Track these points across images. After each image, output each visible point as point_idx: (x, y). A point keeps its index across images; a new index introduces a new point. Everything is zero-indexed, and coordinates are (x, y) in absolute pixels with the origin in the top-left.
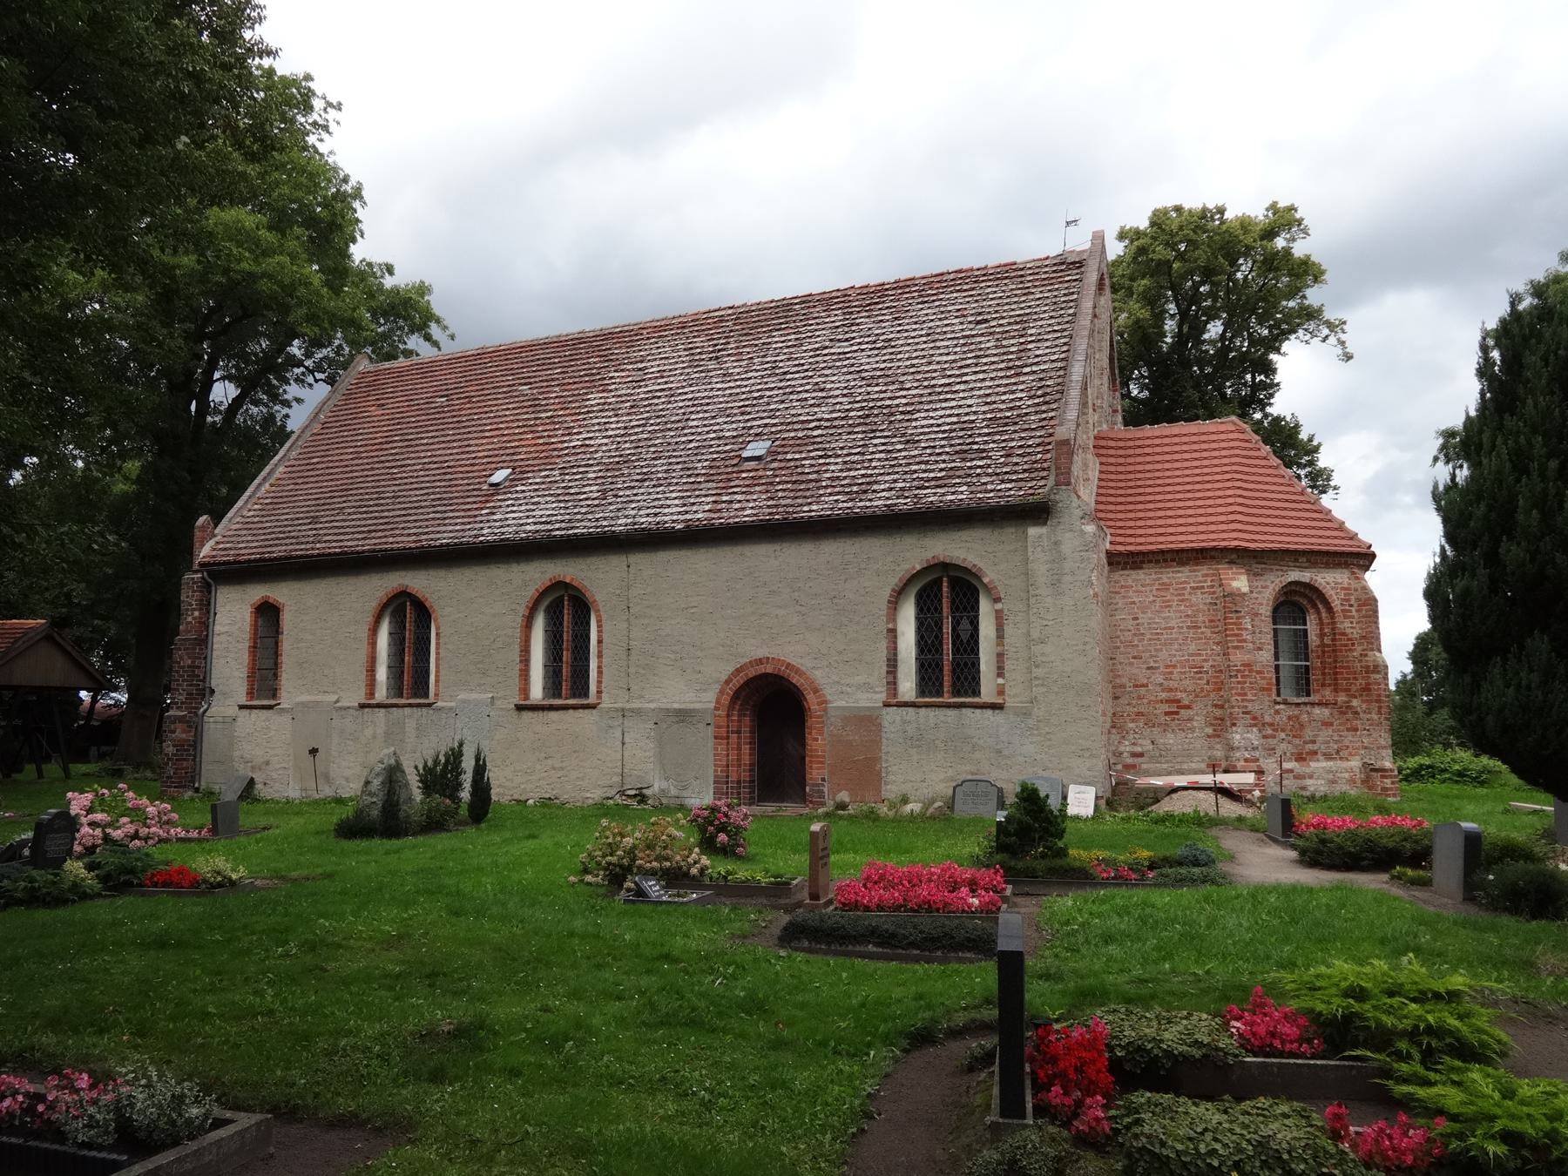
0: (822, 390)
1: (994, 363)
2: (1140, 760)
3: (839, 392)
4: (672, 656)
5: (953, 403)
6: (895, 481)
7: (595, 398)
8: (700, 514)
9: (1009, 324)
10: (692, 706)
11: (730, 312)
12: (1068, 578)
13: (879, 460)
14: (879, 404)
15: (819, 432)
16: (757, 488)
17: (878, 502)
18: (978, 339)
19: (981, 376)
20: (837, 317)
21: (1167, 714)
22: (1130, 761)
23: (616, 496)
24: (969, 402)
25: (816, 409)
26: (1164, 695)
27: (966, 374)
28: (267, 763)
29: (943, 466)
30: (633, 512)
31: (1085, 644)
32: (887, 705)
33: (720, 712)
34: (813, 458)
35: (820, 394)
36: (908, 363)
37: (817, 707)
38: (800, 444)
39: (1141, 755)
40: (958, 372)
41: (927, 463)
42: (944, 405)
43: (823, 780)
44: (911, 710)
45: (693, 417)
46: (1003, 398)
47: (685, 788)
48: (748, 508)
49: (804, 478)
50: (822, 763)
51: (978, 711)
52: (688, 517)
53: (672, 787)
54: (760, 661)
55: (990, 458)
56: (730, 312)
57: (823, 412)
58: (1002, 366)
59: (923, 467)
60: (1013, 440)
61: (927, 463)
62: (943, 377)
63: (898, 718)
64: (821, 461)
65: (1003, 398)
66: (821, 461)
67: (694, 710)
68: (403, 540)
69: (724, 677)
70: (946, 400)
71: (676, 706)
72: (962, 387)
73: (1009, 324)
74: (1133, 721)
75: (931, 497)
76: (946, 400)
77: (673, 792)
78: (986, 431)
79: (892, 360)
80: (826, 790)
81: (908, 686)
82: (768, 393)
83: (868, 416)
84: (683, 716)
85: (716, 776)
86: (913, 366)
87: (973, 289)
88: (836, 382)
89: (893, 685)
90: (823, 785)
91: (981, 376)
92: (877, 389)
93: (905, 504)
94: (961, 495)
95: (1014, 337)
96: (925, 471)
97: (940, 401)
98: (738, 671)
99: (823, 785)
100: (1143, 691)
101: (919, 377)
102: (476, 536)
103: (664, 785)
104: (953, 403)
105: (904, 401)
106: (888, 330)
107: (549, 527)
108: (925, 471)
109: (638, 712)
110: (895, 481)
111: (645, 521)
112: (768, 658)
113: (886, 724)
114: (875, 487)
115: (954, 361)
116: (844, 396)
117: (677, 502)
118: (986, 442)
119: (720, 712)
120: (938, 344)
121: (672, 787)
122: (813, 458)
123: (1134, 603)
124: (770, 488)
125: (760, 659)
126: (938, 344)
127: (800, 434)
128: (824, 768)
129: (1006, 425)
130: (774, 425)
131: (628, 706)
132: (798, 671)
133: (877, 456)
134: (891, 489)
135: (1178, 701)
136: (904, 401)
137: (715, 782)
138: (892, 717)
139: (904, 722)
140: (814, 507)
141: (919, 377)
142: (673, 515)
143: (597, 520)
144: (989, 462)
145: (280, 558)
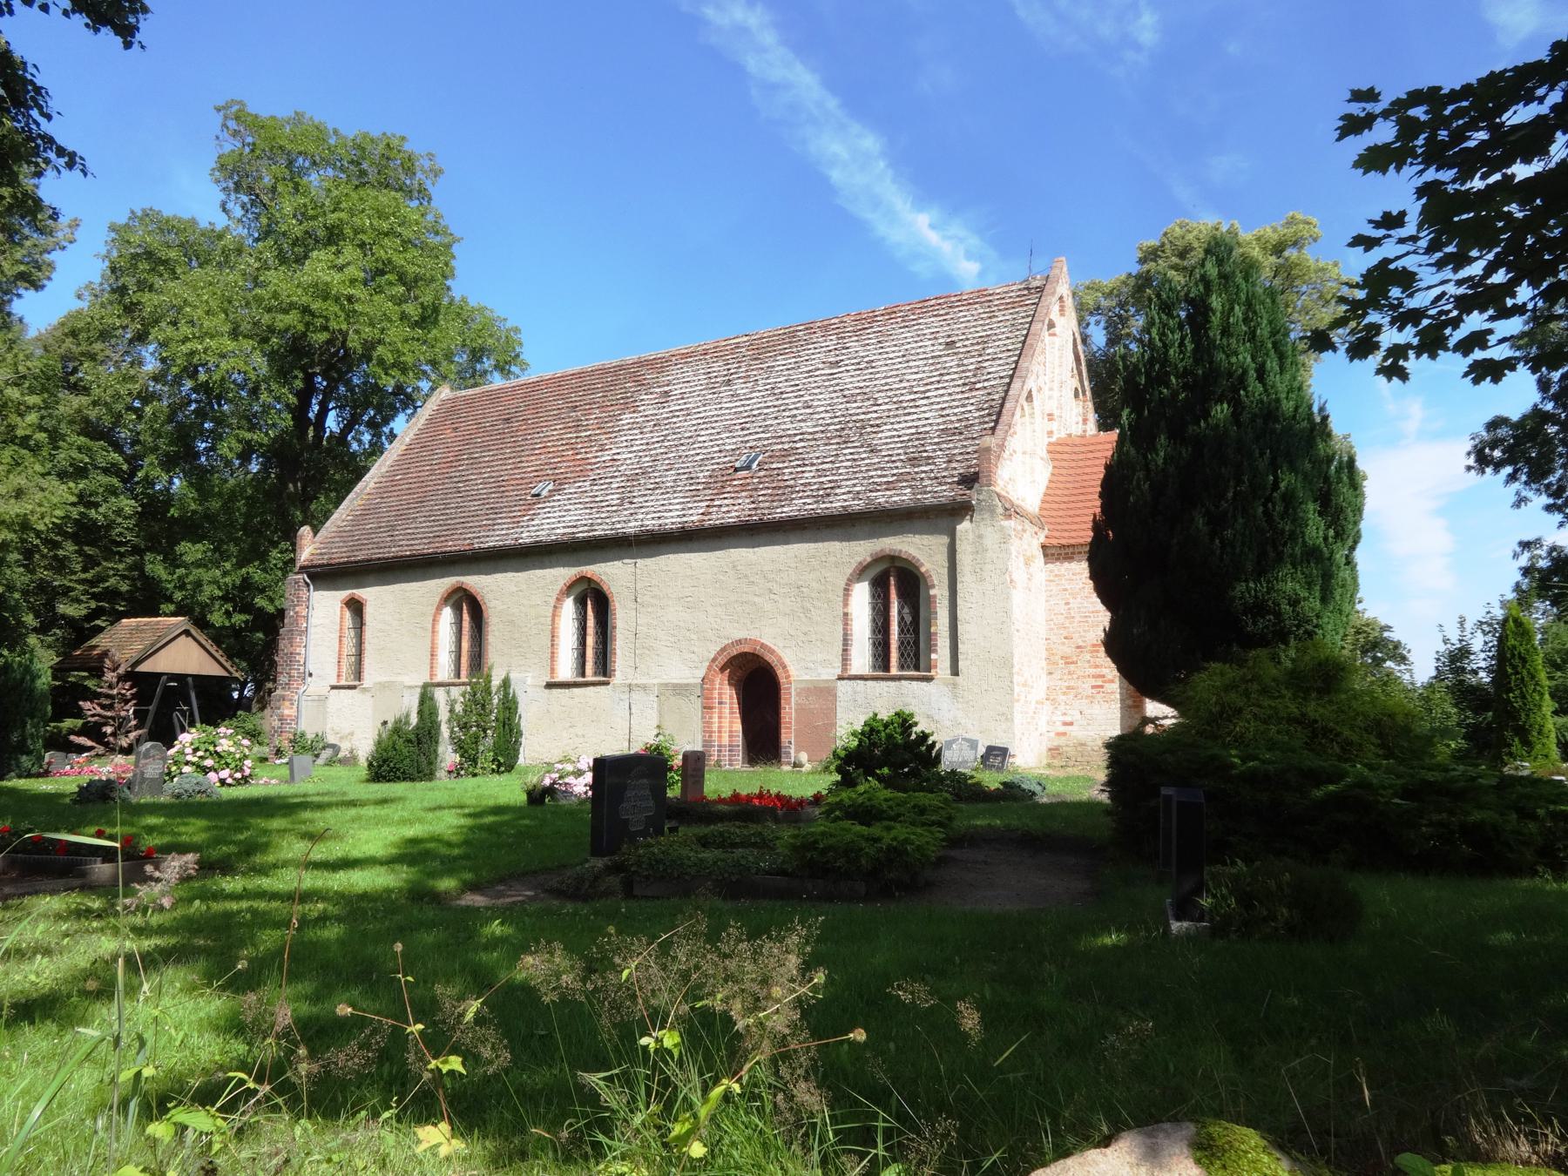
0: (809, 407)
1: (953, 380)
2: (1070, 728)
3: (823, 409)
4: (672, 639)
5: (915, 416)
6: (854, 485)
7: (627, 418)
8: (694, 518)
9: (972, 344)
10: (685, 681)
11: (745, 339)
12: (988, 567)
13: (846, 467)
14: (854, 418)
15: (802, 444)
16: (744, 494)
17: (836, 504)
18: (944, 359)
19: (941, 392)
20: (832, 341)
21: (1093, 687)
22: (1062, 729)
23: (631, 503)
24: (927, 415)
25: (802, 424)
26: (1093, 671)
27: (929, 390)
28: (352, 734)
29: (895, 471)
30: (641, 516)
31: (1003, 623)
32: (840, 678)
34: (793, 467)
35: (808, 411)
36: (883, 382)
38: (785, 454)
39: (1071, 724)
40: (923, 389)
41: (882, 469)
42: (907, 418)
44: (861, 683)
45: (703, 433)
46: (956, 411)
48: (732, 511)
49: (782, 484)
51: (914, 683)
52: (685, 519)
54: (739, 642)
55: (934, 463)
56: (745, 339)
57: (807, 427)
58: (960, 382)
59: (879, 473)
60: (956, 448)
61: (882, 469)
62: (910, 393)
63: (849, 689)
64: (799, 469)
65: (956, 411)
66: (799, 469)
68: (452, 546)
70: (909, 414)
71: (675, 681)
72: (925, 402)
73: (972, 344)
74: (1064, 694)
75: (882, 499)
76: (909, 414)
78: (936, 440)
79: (871, 380)
81: (862, 659)
82: (766, 411)
83: (843, 429)
84: (679, 690)
86: (887, 384)
87: (947, 314)
88: (822, 400)
89: (845, 660)
91: (941, 392)
92: (855, 405)
93: (858, 505)
94: (903, 497)
95: (973, 357)
96: (880, 476)
97: (905, 415)
98: (723, 650)
100: (1072, 667)
101: (889, 394)
102: (516, 539)
104: (915, 416)
105: (875, 415)
106: (872, 353)
107: (574, 530)
108: (880, 476)
109: (644, 688)
110: (854, 485)
111: (651, 524)
113: (839, 694)
114: (838, 491)
115: (921, 379)
116: (827, 411)
117: (678, 507)
118: (935, 451)
120: (911, 364)
122: (793, 467)
123: (1066, 590)
124: (754, 493)
126: (911, 364)
127: (786, 446)
129: (954, 434)
130: (768, 439)
131: (635, 682)
132: (772, 652)
133: (844, 464)
134: (849, 492)
135: (1103, 676)
136: (875, 415)
138: (844, 687)
140: (785, 509)
141: (889, 394)
142: (671, 520)
143: (613, 523)
144: (932, 467)
145: (363, 561)
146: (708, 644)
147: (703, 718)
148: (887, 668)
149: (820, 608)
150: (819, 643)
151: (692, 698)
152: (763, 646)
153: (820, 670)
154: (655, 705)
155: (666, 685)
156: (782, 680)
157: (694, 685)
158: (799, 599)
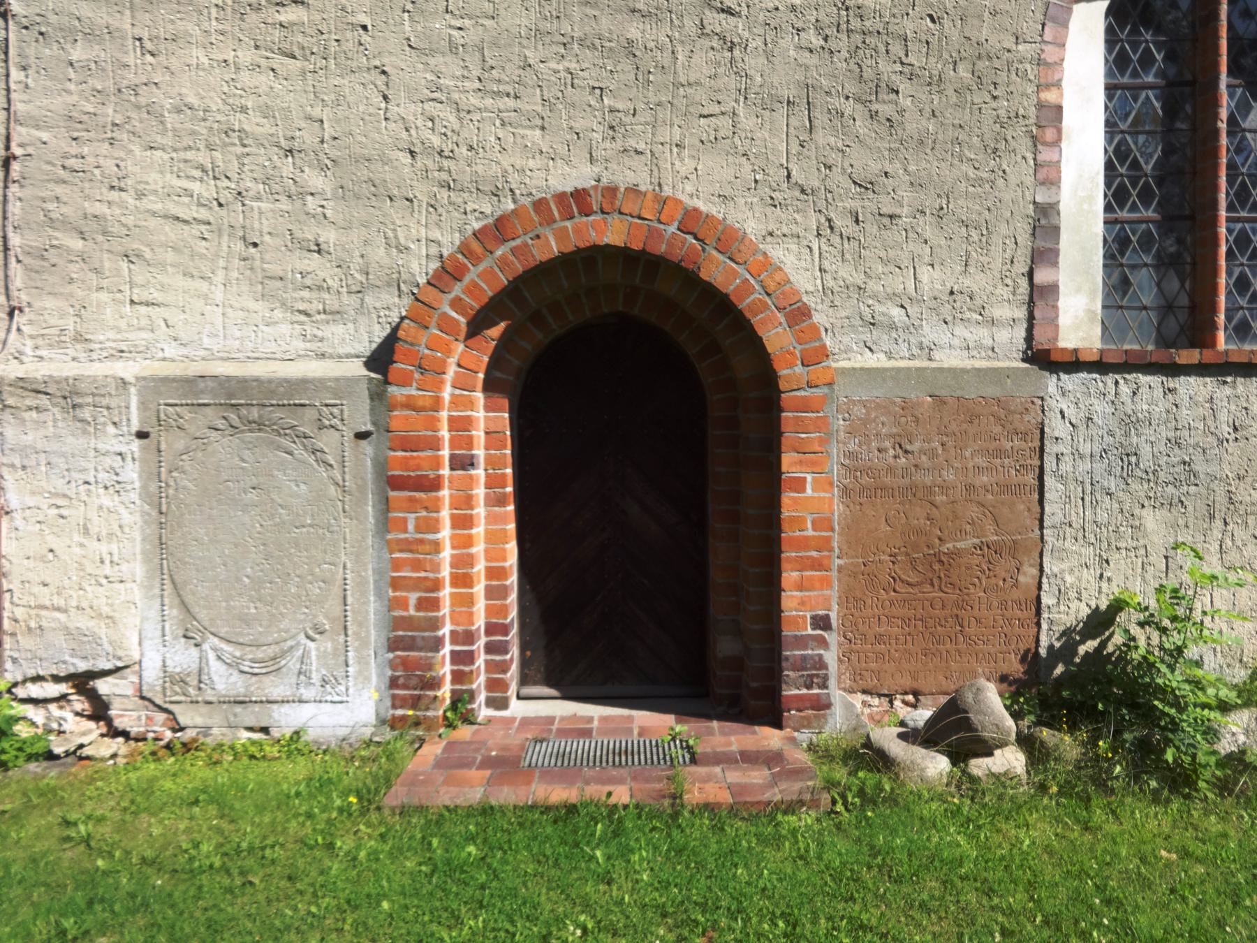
4: (205, 190)
33: (413, 391)
37: (799, 369)
43: (822, 623)
47: (273, 666)
50: (818, 565)
53: (215, 667)
54: (578, 201)
63: (1101, 408)
67: (302, 384)
69: (420, 268)
77: (224, 681)
80: (831, 657)
85: (398, 623)
90: (823, 643)
99: (823, 643)
103: (183, 658)
112: (611, 191)
113: (1056, 427)
119: (413, 391)
121: (215, 667)
125: (580, 196)
128: (826, 582)
132: (729, 241)
137: (393, 645)
139: (1130, 422)
146: (395, 213)
147: (385, 523)
148: (1200, 334)
149: (935, 83)
150: (927, 227)
151: (328, 441)
152: (692, 221)
153: (932, 332)
154: (131, 473)
155: (190, 384)
156: (790, 373)
157: (342, 387)
158: (842, 43)
